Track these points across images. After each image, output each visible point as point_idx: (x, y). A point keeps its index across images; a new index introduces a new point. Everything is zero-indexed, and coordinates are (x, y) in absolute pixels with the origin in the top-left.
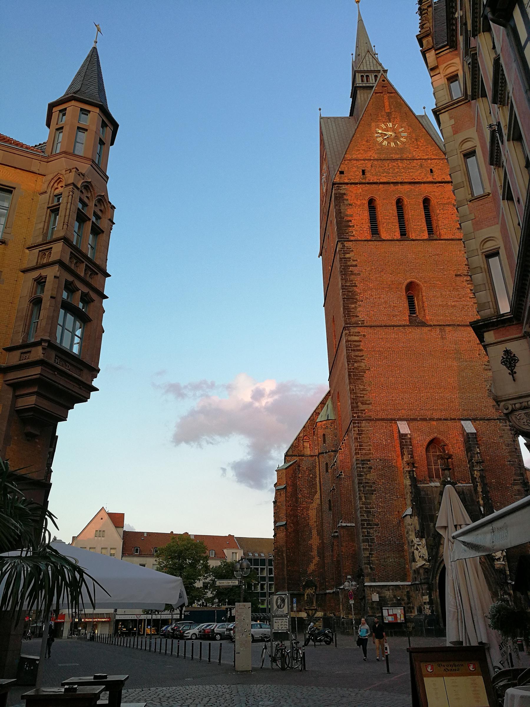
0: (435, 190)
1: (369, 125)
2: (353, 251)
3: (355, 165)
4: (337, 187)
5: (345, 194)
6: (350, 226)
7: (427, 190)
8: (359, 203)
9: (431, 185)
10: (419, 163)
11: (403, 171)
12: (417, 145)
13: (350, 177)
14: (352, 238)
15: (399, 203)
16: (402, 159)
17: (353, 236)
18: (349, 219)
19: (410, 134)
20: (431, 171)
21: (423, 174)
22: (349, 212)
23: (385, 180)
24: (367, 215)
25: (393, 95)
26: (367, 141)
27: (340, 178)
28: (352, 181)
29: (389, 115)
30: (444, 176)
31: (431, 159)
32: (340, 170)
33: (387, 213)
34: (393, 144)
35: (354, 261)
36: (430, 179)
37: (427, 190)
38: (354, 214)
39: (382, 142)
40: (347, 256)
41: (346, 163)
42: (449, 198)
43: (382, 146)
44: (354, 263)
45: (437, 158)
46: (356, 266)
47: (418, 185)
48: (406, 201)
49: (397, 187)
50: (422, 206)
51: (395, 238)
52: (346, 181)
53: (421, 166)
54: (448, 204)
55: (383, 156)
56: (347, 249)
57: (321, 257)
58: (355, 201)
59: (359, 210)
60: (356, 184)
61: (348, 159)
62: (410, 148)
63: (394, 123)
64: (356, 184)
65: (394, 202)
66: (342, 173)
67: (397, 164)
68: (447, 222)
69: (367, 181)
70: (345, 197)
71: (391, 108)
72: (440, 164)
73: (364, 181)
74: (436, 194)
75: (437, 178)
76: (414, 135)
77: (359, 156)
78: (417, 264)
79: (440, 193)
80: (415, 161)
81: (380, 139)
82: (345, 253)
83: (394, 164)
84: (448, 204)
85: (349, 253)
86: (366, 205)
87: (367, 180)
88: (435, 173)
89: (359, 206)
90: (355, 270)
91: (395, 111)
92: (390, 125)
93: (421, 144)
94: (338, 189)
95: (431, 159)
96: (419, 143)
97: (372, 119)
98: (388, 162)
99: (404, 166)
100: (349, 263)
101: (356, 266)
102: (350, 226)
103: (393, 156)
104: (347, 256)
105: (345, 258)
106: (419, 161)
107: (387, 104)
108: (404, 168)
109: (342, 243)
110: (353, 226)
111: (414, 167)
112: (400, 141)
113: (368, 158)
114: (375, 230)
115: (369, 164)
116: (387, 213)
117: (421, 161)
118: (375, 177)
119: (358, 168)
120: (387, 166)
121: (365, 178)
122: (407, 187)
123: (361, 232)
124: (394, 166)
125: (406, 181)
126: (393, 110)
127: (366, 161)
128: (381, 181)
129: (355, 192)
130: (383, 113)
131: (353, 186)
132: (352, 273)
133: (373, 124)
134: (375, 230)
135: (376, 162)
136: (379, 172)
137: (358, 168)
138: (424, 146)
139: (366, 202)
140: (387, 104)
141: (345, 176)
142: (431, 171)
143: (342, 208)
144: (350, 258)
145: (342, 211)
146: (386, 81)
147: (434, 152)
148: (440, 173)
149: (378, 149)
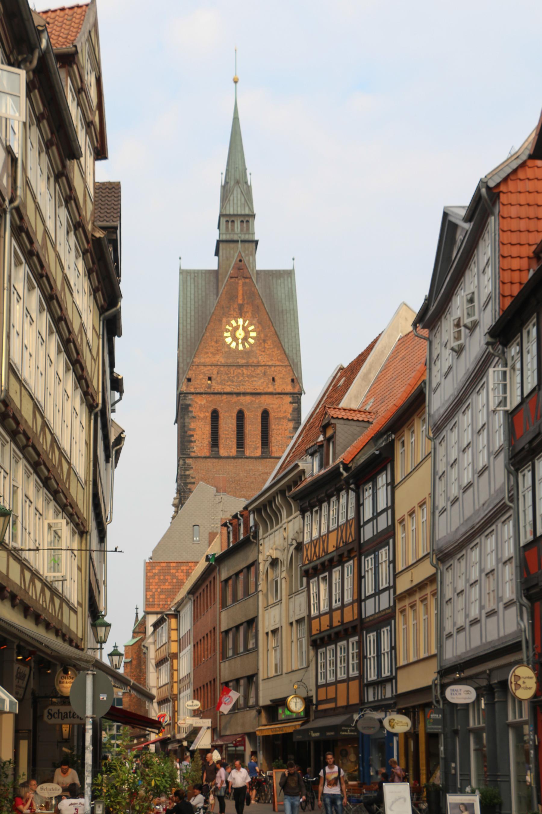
0: (274, 402)
1: (220, 321)
2: (192, 468)
3: (202, 371)
4: (184, 396)
5: (190, 405)
6: (192, 442)
7: (267, 402)
8: (202, 415)
9: (271, 396)
10: (263, 371)
11: (247, 379)
12: (264, 348)
13: (196, 386)
14: (193, 455)
15: (240, 416)
16: (247, 366)
17: (194, 452)
18: (192, 433)
19: (258, 334)
20: (273, 379)
21: (265, 383)
22: (192, 425)
23: (228, 389)
24: (208, 429)
25: (247, 280)
26: (216, 342)
27: (187, 386)
28: (198, 391)
29: (241, 307)
30: (284, 386)
31: (275, 366)
32: (188, 377)
33: (228, 426)
34: (241, 347)
35: (193, 478)
36: (271, 390)
37: (267, 402)
38: (197, 428)
39: (230, 344)
40: (187, 473)
41: (194, 368)
42: (285, 412)
43: (230, 348)
44: (193, 480)
45: (281, 364)
46: (194, 483)
47: (259, 396)
48: (247, 413)
49: (239, 398)
50: (259, 420)
51: (231, 455)
52: (192, 390)
53: (265, 374)
55: (230, 361)
56: (188, 465)
57: (176, 424)
58: (199, 414)
59: (201, 423)
60: (201, 394)
61: (197, 364)
62: (257, 351)
63: (245, 319)
64: (201, 394)
65: (234, 415)
66: (189, 380)
67: (242, 371)
68: (280, 438)
69: (211, 391)
70: (190, 409)
71: (243, 299)
72: (283, 372)
73: (209, 391)
74: (274, 406)
75: (277, 389)
76: (262, 335)
77: (208, 361)
78: (248, 483)
79: (277, 406)
80: (260, 368)
81: (229, 340)
82: (186, 470)
83: (240, 371)
84: (283, 418)
85: (188, 470)
86: (209, 419)
87: (212, 390)
88: (276, 383)
89: (202, 419)
91: (248, 303)
92: (240, 321)
93: (268, 347)
94: (184, 399)
95: (275, 366)
96: (266, 345)
97: (223, 314)
98: (234, 368)
99: (249, 373)
100: (188, 481)
101: (194, 483)
102: (192, 442)
103: (239, 360)
104: (187, 473)
105: (185, 475)
106: (264, 367)
107: (240, 293)
108: (248, 376)
109: (184, 460)
110: (195, 441)
111: (258, 374)
113: (215, 362)
116: (228, 426)
117: (265, 367)
118: (220, 387)
119: (204, 374)
120: (232, 373)
122: (248, 398)
123: (202, 448)
124: (239, 373)
125: (248, 391)
126: (245, 302)
127: (213, 367)
128: (226, 391)
129: (199, 403)
130: (236, 306)
131: (199, 396)
133: (224, 320)
135: (222, 369)
136: (224, 380)
137: (204, 374)
138: (271, 349)
139: (209, 415)
140: (240, 293)
141: (192, 385)
143: (187, 420)
144: (189, 475)
145: (186, 424)
146: (243, 262)
147: (279, 358)
148: (281, 383)
149: (226, 352)
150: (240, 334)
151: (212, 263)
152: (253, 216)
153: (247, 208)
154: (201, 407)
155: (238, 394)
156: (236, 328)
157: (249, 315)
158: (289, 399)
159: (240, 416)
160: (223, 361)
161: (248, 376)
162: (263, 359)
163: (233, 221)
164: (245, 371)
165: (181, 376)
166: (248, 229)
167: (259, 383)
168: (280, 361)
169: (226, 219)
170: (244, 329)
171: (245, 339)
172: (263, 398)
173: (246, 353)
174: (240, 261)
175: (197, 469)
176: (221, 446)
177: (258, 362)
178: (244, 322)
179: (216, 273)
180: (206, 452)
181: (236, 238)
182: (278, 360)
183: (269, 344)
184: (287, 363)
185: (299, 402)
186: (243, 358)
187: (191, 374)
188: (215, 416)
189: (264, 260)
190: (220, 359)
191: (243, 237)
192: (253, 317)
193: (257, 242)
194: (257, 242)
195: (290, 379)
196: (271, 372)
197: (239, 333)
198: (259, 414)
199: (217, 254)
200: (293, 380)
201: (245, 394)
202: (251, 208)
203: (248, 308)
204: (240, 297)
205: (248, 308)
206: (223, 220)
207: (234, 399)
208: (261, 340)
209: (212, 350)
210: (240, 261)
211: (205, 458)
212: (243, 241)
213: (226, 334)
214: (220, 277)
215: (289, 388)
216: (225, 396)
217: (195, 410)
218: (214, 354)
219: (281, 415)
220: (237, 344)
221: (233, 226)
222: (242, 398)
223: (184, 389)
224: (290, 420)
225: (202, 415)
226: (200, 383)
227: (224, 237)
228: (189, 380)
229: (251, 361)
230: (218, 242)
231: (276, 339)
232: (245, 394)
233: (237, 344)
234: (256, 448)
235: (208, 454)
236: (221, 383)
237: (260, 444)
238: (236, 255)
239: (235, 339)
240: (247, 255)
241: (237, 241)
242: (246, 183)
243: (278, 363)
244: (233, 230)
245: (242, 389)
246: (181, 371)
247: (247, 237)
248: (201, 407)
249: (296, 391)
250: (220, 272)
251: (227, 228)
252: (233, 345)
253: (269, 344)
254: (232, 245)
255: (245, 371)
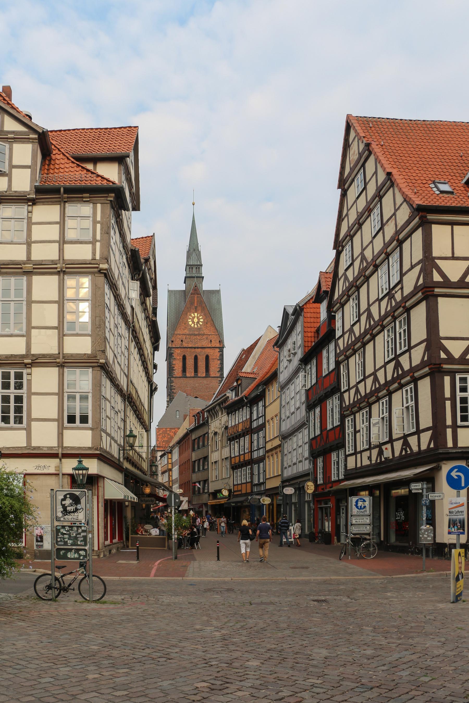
1: (187, 314)
5: (173, 353)
7: (208, 351)
8: (178, 358)
14: (174, 376)
15: (196, 358)
19: (204, 320)
20: (211, 341)
22: (174, 363)
23: (190, 346)
25: (199, 295)
26: (185, 324)
29: (196, 308)
33: (190, 362)
34: (196, 326)
36: (210, 346)
37: (208, 351)
40: (172, 384)
48: (199, 357)
52: (174, 346)
53: (207, 338)
54: (215, 359)
55: (191, 332)
65: (193, 358)
66: (172, 341)
69: (183, 346)
70: (173, 355)
71: (197, 304)
73: (181, 346)
74: (211, 354)
77: (181, 332)
81: (190, 323)
82: (171, 383)
84: (215, 359)
86: (182, 359)
90: (174, 391)
92: (196, 314)
104: (172, 384)
107: (196, 301)
108: (199, 340)
112: (200, 324)
114: (184, 370)
115: (184, 337)
116: (190, 362)
121: (182, 345)
122: (199, 350)
130: (194, 307)
132: (173, 393)
133: (188, 314)
134: (184, 370)
137: (179, 339)
139: (181, 357)
140: (196, 301)
142: (211, 341)
143: (172, 360)
150: (196, 320)
151: (182, 287)
152: (202, 265)
153: (199, 262)
154: (178, 354)
155: (195, 348)
156: (194, 317)
157: (200, 311)
158: (218, 350)
159: (196, 358)
160: (188, 333)
161: (199, 340)
162: (206, 332)
163: (192, 268)
164: (198, 337)
165: (169, 340)
166: (199, 271)
167: (204, 343)
168: (214, 332)
169: (189, 267)
170: (197, 318)
171: (198, 322)
172: (206, 349)
173: (199, 329)
174: (196, 286)
175: (176, 383)
176: (187, 372)
177: (204, 333)
178: (198, 314)
179: (184, 291)
180: (180, 375)
181: (193, 275)
182: (213, 332)
183: (209, 325)
184: (217, 334)
185: (222, 351)
186: (197, 331)
187: (173, 339)
188: (184, 358)
189: (206, 286)
190: (186, 332)
191: (197, 275)
192: (202, 312)
193: (203, 277)
194: (203, 277)
195: (218, 341)
196: (210, 337)
197: (195, 320)
198: (204, 357)
199: (185, 282)
200: (220, 341)
201: (198, 348)
202: (201, 262)
203: (199, 308)
204: (196, 303)
205: (199, 308)
206: (188, 267)
207: (193, 350)
208: (205, 323)
209: (183, 327)
210: (196, 286)
211: (180, 377)
212: (197, 277)
213: (189, 320)
214: (186, 293)
215: (218, 345)
216: (189, 349)
217: (175, 356)
218: (184, 329)
219: (215, 357)
220: (194, 325)
221: (192, 270)
222: (196, 349)
223: (170, 346)
224: (218, 360)
225: (178, 358)
226: (177, 343)
227: (188, 275)
228: (172, 341)
229: (200, 332)
230: (186, 278)
231: (212, 322)
232: (198, 348)
233: (194, 325)
234: (203, 373)
235: (181, 376)
236: (187, 343)
237: (205, 371)
238: (194, 283)
239: (193, 322)
240: (199, 283)
241: (194, 277)
242: (198, 250)
243: (213, 334)
244: (192, 272)
245: (196, 346)
246: (169, 337)
247: (199, 275)
248: (178, 354)
249: (221, 346)
250: (186, 291)
251: (190, 271)
252: (193, 325)
253: (209, 325)
254: (192, 279)
255: (198, 337)
